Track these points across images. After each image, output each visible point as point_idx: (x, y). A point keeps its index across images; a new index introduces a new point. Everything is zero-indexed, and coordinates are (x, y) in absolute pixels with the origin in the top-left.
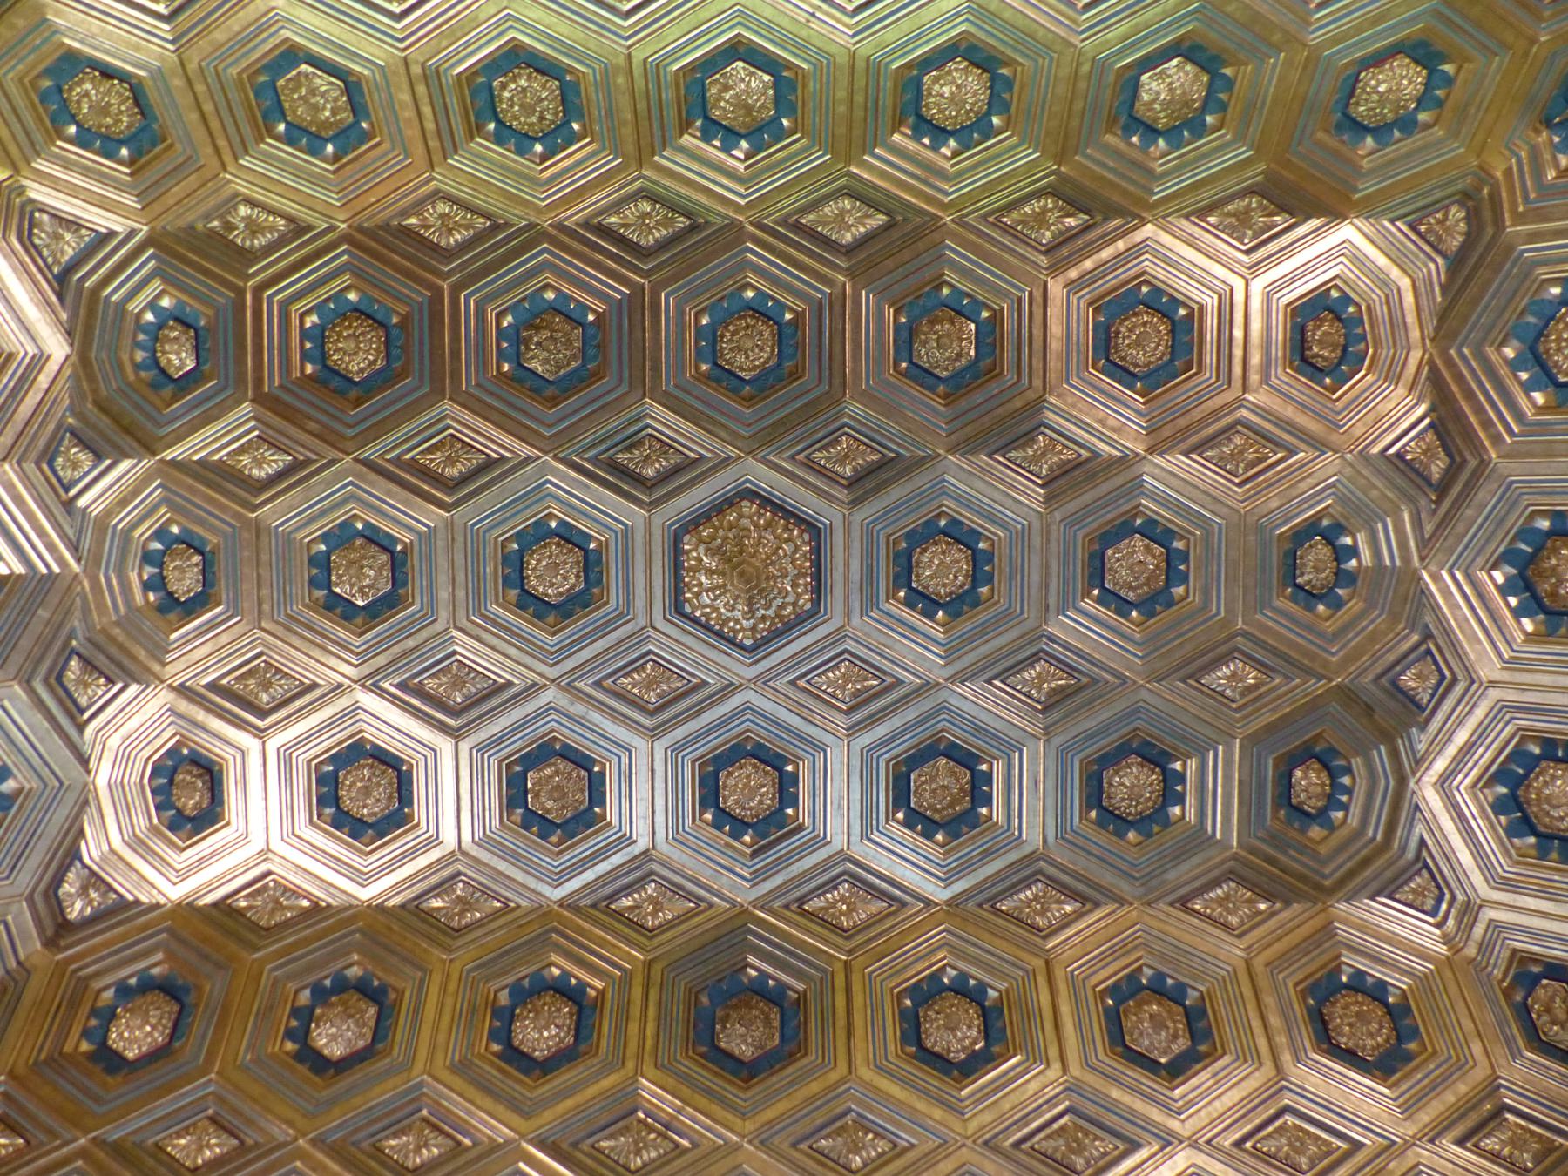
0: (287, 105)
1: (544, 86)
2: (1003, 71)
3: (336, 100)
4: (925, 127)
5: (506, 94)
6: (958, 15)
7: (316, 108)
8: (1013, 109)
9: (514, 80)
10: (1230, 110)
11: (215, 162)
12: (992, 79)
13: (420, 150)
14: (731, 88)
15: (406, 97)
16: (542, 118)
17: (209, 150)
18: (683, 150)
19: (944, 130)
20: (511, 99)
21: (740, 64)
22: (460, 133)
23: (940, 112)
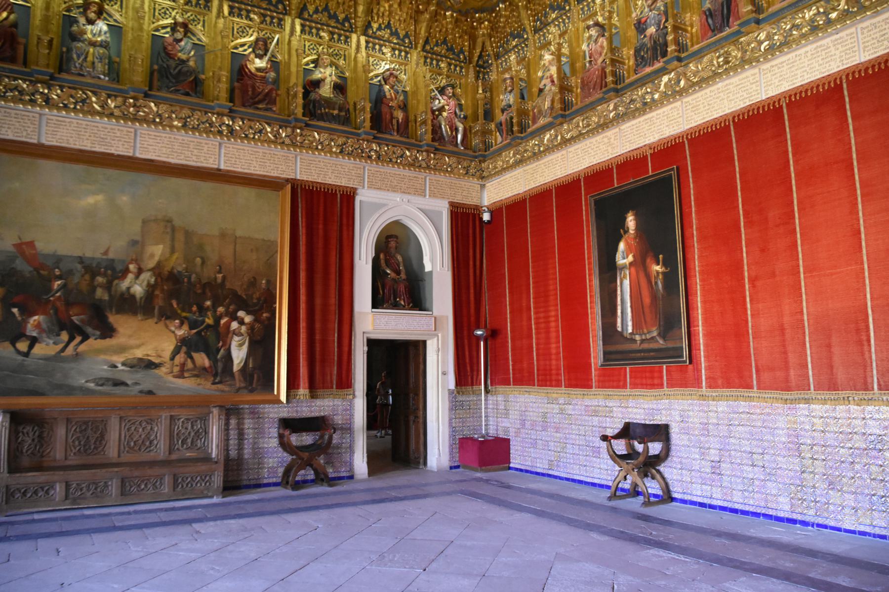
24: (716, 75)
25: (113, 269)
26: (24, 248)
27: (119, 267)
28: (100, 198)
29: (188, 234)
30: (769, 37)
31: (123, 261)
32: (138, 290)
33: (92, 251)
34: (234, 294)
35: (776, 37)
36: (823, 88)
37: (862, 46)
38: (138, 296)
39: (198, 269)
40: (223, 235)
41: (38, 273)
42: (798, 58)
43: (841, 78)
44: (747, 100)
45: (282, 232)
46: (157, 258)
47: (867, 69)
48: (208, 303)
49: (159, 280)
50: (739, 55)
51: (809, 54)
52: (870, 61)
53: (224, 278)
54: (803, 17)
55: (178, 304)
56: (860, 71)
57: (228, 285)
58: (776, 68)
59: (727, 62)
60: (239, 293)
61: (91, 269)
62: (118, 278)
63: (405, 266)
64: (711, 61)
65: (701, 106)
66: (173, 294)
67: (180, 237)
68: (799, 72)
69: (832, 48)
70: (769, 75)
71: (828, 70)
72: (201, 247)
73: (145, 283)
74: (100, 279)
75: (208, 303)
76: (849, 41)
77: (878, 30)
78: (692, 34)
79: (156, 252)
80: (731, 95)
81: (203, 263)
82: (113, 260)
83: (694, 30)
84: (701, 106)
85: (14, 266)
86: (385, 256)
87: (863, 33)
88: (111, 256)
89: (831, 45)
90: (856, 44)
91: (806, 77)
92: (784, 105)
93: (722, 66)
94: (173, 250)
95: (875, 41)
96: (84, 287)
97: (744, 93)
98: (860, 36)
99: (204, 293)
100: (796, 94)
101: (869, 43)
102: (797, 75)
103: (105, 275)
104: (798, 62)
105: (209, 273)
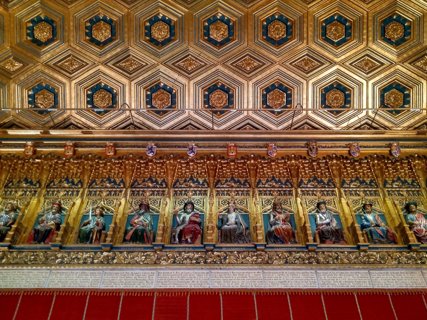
0: (344, 31)
1: (272, 35)
2: (148, 38)
3: (330, 32)
4: (168, 22)
5: (282, 33)
6: (162, 54)
7: (336, 30)
8: (144, 27)
9: (280, 37)
10: (84, 28)
11: (370, 15)
12: (151, 36)
13: (310, 18)
14: (221, 35)
15: (310, 33)
16: (274, 26)
17: (370, 18)
18: (236, 16)
19: (163, 21)
20: (281, 32)
21: (219, 41)
22: (297, 22)
23: (164, 27)
24: (26, 264)
30: (63, 258)
35: (66, 259)
36: (78, 294)
37: (102, 281)
42: (72, 274)
43: (88, 293)
44: (36, 285)
47: (101, 293)
50: (43, 259)
51: (78, 274)
52: (103, 289)
54: (83, 256)
56: (97, 292)
58: (59, 274)
59: (35, 260)
64: (27, 256)
65: (9, 278)
68: (69, 281)
69: (89, 276)
70: (54, 276)
71: (83, 286)
76: (98, 276)
77: (111, 276)
78: (22, 236)
80: (29, 279)
83: (24, 235)
84: (9, 278)
87: (105, 275)
89: (89, 274)
90: (100, 279)
91: (72, 285)
92: (55, 296)
93: (32, 261)
95: (109, 281)
97: (37, 281)
98: (104, 276)
100: (63, 292)
101: (106, 281)
102: (67, 282)
104: (71, 276)
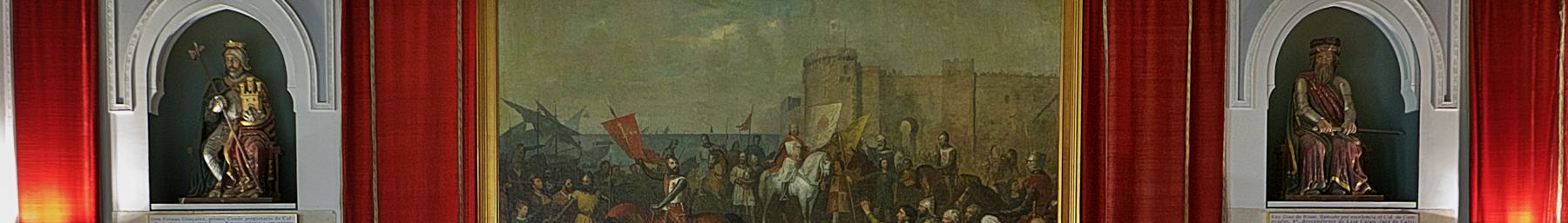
25: (760, 152)
26: (620, 127)
27: (770, 149)
28: (731, 28)
29: (885, 78)
31: (776, 137)
32: (803, 186)
33: (724, 125)
34: (976, 184)
38: (802, 197)
39: (906, 142)
40: (950, 75)
41: (643, 167)
45: (1068, 56)
46: (832, 128)
48: (927, 204)
49: (837, 166)
53: (954, 154)
55: (871, 209)
57: (962, 168)
60: (984, 183)
61: (725, 155)
62: (768, 167)
63: (1356, 104)
66: (864, 190)
67: (871, 84)
72: (909, 100)
73: (815, 172)
74: (739, 171)
75: (927, 204)
79: (831, 115)
81: (914, 130)
82: (759, 136)
85: (607, 158)
86: (1309, 85)
88: (754, 130)
94: (859, 112)
96: (714, 186)
99: (918, 185)
103: (746, 163)
105: (926, 147)
